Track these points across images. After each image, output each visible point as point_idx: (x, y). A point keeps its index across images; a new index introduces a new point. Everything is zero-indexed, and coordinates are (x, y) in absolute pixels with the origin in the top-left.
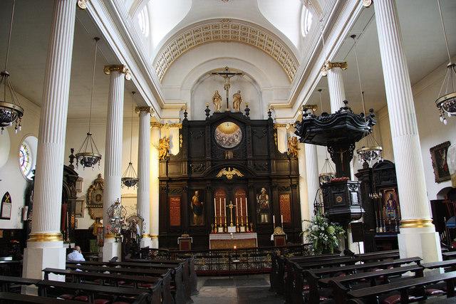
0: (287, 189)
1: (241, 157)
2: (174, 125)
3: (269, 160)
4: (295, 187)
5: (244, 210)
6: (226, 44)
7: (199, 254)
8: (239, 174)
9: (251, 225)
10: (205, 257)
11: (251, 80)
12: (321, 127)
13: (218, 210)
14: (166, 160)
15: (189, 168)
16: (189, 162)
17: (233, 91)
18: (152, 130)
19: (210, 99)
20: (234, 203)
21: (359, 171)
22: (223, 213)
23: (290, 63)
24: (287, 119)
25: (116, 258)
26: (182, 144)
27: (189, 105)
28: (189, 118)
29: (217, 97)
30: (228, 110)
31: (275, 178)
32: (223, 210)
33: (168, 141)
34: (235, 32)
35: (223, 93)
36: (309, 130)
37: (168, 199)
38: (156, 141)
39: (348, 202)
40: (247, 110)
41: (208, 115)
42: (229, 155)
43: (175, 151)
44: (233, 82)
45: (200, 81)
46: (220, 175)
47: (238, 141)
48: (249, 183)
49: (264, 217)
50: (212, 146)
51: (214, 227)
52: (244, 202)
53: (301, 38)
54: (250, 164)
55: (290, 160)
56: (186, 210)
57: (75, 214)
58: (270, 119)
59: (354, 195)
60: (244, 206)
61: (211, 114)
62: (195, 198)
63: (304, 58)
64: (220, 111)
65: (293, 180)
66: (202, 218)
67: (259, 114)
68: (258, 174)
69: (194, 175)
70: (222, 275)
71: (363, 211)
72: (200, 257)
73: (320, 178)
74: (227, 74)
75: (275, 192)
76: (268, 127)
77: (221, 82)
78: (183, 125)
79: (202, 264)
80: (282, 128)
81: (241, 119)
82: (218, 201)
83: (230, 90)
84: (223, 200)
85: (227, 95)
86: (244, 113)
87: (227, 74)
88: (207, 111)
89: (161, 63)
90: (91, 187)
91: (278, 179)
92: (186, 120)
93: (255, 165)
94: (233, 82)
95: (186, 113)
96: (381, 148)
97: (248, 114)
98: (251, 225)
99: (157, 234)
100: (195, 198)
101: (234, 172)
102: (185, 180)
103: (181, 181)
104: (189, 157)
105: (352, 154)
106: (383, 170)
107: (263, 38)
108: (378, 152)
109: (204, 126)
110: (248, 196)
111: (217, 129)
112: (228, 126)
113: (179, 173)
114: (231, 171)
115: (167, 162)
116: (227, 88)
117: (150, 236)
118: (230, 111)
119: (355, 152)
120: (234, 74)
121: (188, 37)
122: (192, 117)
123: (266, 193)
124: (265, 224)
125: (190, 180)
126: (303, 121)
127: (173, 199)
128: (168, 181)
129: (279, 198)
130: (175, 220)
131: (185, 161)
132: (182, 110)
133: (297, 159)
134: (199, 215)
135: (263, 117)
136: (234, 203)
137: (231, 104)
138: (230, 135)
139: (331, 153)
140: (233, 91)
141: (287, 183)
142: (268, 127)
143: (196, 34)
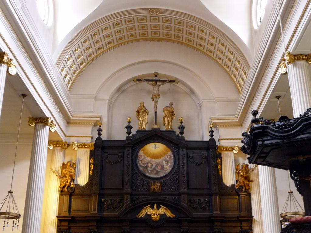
2: (83, 146)
3: (210, 195)
6: (156, 43)
8: (169, 214)
11: (187, 90)
12: (278, 137)
14: (69, 191)
15: (101, 204)
16: (101, 195)
17: (163, 103)
23: (239, 66)
26: (93, 170)
27: (105, 119)
28: (104, 137)
29: (142, 111)
30: (156, 127)
33: (73, 165)
34: (167, 28)
35: (150, 105)
40: (182, 128)
41: (129, 133)
42: (156, 187)
43: (83, 180)
45: (121, 90)
46: (142, 214)
47: (168, 168)
53: (253, 33)
55: (239, 195)
58: (212, 140)
61: (133, 131)
65: (244, 224)
68: (196, 214)
69: (106, 214)
74: (156, 80)
76: (211, 151)
77: (149, 92)
78: (96, 145)
80: (228, 153)
81: (173, 140)
83: (159, 102)
85: (156, 107)
86: (177, 132)
87: (156, 81)
88: (129, 128)
89: (69, 63)
91: (222, 221)
92: (99, 139)
93: (190, 201)
94: (164, 93)
95: (100, 131)
97: (182, 133)
101: (162, 211)
102: (93, 220)
103: (88, 221)
107: (202, 35)
109: (123, 148)
111: (141, 153)
112: (155, 148)
113: (87, 210)
114: (158, 208)
115: (71, 195)
116: (155, 98)
118: (158, 129)
120: (166, 81)
121: (106, 33)
122: (108, 136)
126: (252, 129)
131: (95, 194)
132: (95, 125)
133: (249, 195)
135: (203, 137)
138: (158, 161)
139: (296, 181)
140: (163, 103)
142: (211, 151)
143: (117, 28)
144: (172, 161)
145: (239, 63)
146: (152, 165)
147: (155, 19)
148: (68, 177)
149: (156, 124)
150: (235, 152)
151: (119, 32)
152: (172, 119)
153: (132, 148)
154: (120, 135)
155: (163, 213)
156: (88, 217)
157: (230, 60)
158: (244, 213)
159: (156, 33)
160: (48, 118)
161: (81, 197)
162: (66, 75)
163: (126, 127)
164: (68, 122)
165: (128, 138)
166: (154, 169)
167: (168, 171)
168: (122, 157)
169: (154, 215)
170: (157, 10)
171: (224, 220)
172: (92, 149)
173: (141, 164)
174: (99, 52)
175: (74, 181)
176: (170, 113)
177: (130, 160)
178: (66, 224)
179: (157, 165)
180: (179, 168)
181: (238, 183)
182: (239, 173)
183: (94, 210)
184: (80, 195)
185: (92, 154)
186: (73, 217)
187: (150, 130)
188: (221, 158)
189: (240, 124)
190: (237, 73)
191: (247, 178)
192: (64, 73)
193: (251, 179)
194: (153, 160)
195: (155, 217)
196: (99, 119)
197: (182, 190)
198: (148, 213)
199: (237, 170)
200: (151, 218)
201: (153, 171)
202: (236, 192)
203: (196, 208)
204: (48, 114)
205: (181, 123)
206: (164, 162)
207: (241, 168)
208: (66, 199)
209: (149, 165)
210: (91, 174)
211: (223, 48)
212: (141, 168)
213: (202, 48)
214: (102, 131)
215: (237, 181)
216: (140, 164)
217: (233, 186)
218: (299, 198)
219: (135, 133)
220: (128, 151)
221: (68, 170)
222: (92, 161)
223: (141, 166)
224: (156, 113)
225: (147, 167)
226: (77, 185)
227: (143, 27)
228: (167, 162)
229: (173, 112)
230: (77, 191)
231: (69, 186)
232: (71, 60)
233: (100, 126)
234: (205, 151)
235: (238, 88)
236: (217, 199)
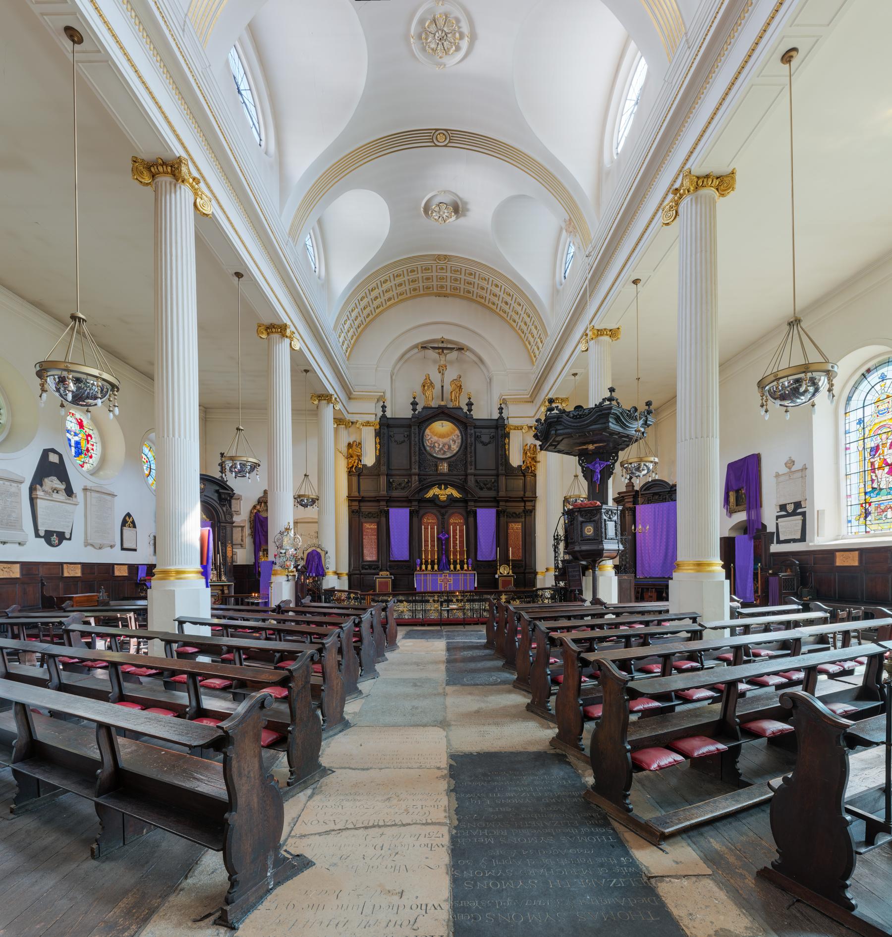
2: (368, 424)
3: (497, 475)
4: (529, 513)
5: (461, 542)
6: (442, 299)
7: (401, 598)
8: (456, 494)
10: (408, 601)
13: (426, 541)
14: (356, 472)
15: (389, 484)
17: (451, 374)
18: (336, 430)
19: (419, 389)
21: (619, 493)
22: (433, 546)
23: (535, 332)
24: (524, 418)
25: (289, 602)
27: (388, 396)
28: (389, 414)
29: (427, 384)
30: (443, 403)
31: (502, 501)
34: (456, 280)
35: (436, 378)
36: (553, 431)
39: (599, 535)
40: (470, 404)
41: (414, 410)
43: (369, 459)
44: (451, 362)
46: (430, 494)
47: (455, 448)
51: (421, 564)
52: (461, 531)
54: (471, 480)
55: (524, 476)
57: (233, 545)
58: (501, 418)
59: (611, 526)
60: (461, 536)
61: (419, 408)
63: (555, 323)
64: (434, 404)
65: (528, 504)
67: (484, 411)
69: (395, 494)
70: (429, 625)
71: (621, 547)
72: (401, 601)
73: (566, 500)
74: (442, 347)
76: (499, 429)
77: (435, 362)
79: (404, 609)
82: (426, 529)
83: (446, 373)
84: (432, 528)
85: (442, 381)
86: (465, 409)
87: (443, 349)
88: (414, 404)
89: (346, 327)
90: (255, 507)
91: (507, 501)
92: (384, 416)
93: (476, 481)
94: (451, 362)
95: (384, 407)
96: (656, 460)
97: (470, 410)
99: (347, 571)
101: (451, 491)
102: (383, 500)
103: (378, 501)
104: (389, 468)
105: (613, 469)
106: (655, 494)
108: (651, 466)
109: (410, 426)
111: (427, 431)
114: (445, 489)
115: (359, 475)
116: (442, 370)
117: (336, 573)
118: (445, 406)
119: (617, 465)
127: (367, 526)
128: (360, 501)
131: (383, 474)
133: (535, 476)
137: (447, 395)
138: (445, 440)
140: (451, 374)
141: (519, 508)
142: (499, 429)
144: (460, 441)
145: (536, 328)
147: (442, 269)
148: (355, 457)
151: (400, 285)
154: (407, 413)
157: (525, 324)
158: (528, 494)
159: (442, 287)
162: (344, 342)
164: (350, 398)
165: (414, 416)
166: (442, 449)
168: (409, 436)
170: (445, 257)
171: (508, 500)
172: (378, 427)
174: (378, 311)
178: (357, 503)
180: (466, 448)
185: (378, 434)
188: (509, 438)
190: (532, 340)
192: (341, 340)
193: (538, 459)
195: (443, 498)
197: (469, 471)
200: (439, 498)
203: (481, 489)
208: (355, 479)
209: (436, 445)
211: (518, 309)
212: (428, 448)
213: (494, 307)
216: (427, 444)
218: (585, 484)
220: (415, 429)
221: (353, 450)
222: (378, 441)
225: (434, 447)
226: (364, 466)
227: (428, 279)
228: (454, 441)
232: (348, 323)
234: (493, 430)
235: (532, 358)
236: (502, 479)
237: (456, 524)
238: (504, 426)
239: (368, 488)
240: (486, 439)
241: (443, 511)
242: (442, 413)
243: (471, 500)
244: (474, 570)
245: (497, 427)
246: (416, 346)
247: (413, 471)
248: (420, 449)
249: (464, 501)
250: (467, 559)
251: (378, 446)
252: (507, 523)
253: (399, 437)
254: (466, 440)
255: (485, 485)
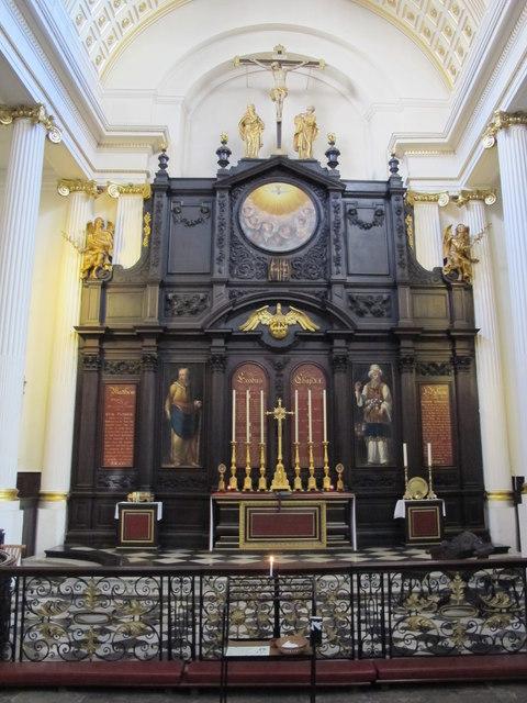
0: (439, 370)
1: (304, 277)
2: (129, 190)
3: (394, 286)
4: (465, 363)
5: (318, 427)
8: (307, 323)
9: (340, 469)
11: (344, 89)
13: (241, 424)
14: (101, 278)
17: (292, 111)
20: (289, 406)
22: (256, 435)
26: (150, 239)
28: (174, 171)
31: (408, 337)
32: (256, 424)
37: (100, 387)
38: (77, 229)
40: (333, 153)
41: (223, 163)
42: (281, 271)
43: (128, 254)
45: (210, 85)
46: (253, 322)
47: (305, 232)
48: (337, 342)
49: (377, 450)
50: (234, 244)
51: (228, 475)
52: (317, 402)
55: (449, 288)
56: (150, 429)
61: (233, 161)
62: (177, 389)
64: (263, 154)
65: (459, 345)
66: (196, 446)
67: (362, 166)
69: (177, 323)
75: (409, 379)
76: (393, 198)
78: (155, 188)
81: (317, 181)
84: (255, 397)
85: (279, 114)
86: (324, 161)
87: (281, 62)
88: (223, 152)
92: (162, 174)
93: (351, 299)
95: (163, 160)
97: (333, 164)
98: (340, 469)
100: (177, 389)
102: (149, 336)
103: (139, 337)
109: (212, 192)
110: (330, 387)
111: (248, 202)
114: (284, 313)
115: (104, 286)
123: (385, 379)
124: (377, 469)
125: (164, 336)
127: (115, 390)
129: (419, 394)
130: (118, 456)
131: (153, 283)
133: (469, 289)
134: (186, 435)
136: (289, 406)
138: (285, 218)
142: (393, 198)
144: (314, 219)
146: (272, 227)
149: (279, 146)
150: (441, 203)
152: (313, 138)
153: (230, 192)
154: (208, 169)
155: (295, 322)
156: (140, 328)
158: (459, 324)
160: (38, 106)
161: (125, 290)
163: (219, 152)
167: (304, 240)
168: (210, 212)
169: (277, 325)
171: (420, 336)
172: (149, 194)
173: (250, 225)
175: (110, 259)
176: (309, 125)
177: (226, 215)
178: (95, 343)
179: (281, 228)
180: (327, 232)
181: (449, 263)
182: (450, 243)
183: (152, 317)
184: (124, 286)
186: (107, 329)
187: (268, 157)
188: (412, 215)
189: (451, 148)
191: (465, 254)
193: (474, 256)
194: (275, 216)
196: (162, 134)
197: (335, 277)
198: (263, 323)
199: (446, 238)
200: (270, 333)
201: (273, 238)
202: (445, 282)
203: (361, 314)
204: (38, 97)
205: (332, 143)
206: (296, 220)
207: (454, 233)
208: (96, 293)
209: (266, 227)
210: (146, 244)
212: (248, 234)
214: (167, 159)
215: (445, 261)
216: (246, 225)
217: (438, 270)
219: (236, 165)
222: (148, 218)
223: (249, 229)
224: (279, 123)
225: (261, 231)
226: (118, 267)
228: (303, 221)
229: (315, 124)
230: (117, 279)
231: (99, 269)
233: (164, 150)
234: (381, 201)
236: (405, 294)
237: (309, 387)
238: (402, 191)
239: (123, 310)
240: (366, 216)
241: (279, 358)
242: (278, 169)
243: (339, 336)
244: (348, 489)
245: (387, 196)
246: (231, 65)
247: (217, 275)
248: (232, 235)
249: (327, 339)
250: (332, 465)
251: (148, 229)
252: (419, 385)
253: (192, 214)
254: (327, 216)
255: (369, 305)
